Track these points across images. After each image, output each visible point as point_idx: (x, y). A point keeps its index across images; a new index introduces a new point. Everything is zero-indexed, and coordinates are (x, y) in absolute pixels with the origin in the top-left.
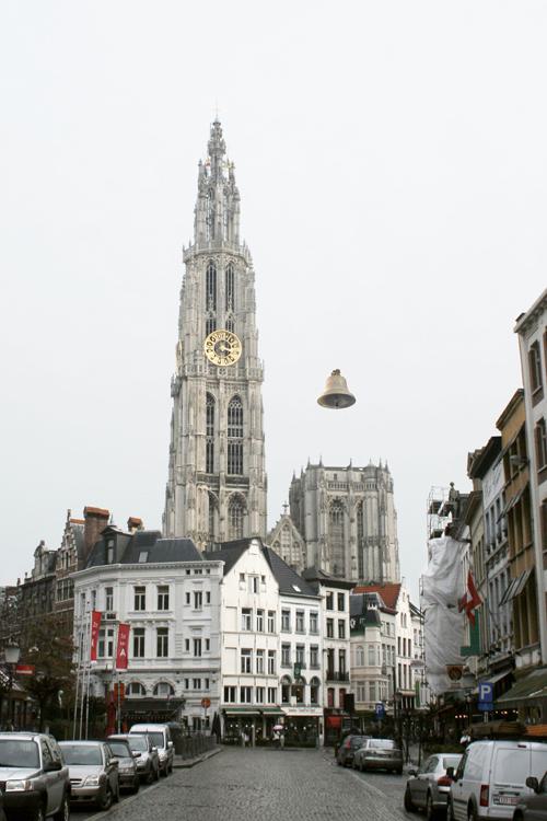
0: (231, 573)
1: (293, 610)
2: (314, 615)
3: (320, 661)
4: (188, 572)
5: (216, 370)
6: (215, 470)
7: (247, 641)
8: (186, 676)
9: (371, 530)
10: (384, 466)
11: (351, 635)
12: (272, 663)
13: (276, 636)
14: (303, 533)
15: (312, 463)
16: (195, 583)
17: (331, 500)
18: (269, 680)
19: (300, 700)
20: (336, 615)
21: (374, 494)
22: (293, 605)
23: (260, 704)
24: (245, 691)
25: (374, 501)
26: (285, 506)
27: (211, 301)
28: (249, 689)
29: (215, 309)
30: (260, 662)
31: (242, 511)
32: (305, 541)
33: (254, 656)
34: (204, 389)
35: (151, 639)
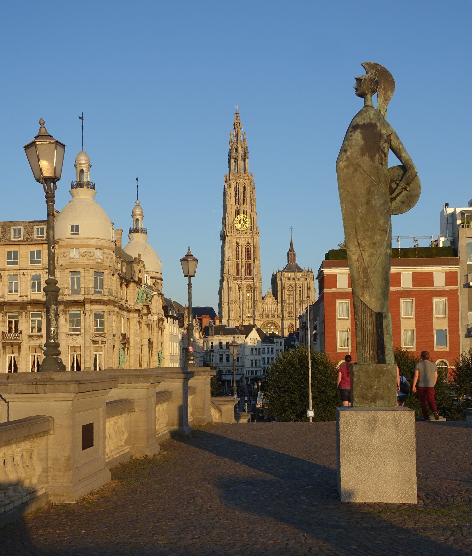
0: (247, 338)
2: (272, 348)
5: (240, 232)
6: (240, 274)
7: (253, 357)
10: (310, 270)
12: (260, 363)
13: (261, 355)
14: (276, 299)
15: (280, 270)
20: (279, 348)
21: (306, 282)
24: (252, 372)
25: (306, 285)
29: (239, 204)
30: (256, 363)
32: (277, 302)
33: (254, 362)
34: (235, 240)
35: (224, 357)
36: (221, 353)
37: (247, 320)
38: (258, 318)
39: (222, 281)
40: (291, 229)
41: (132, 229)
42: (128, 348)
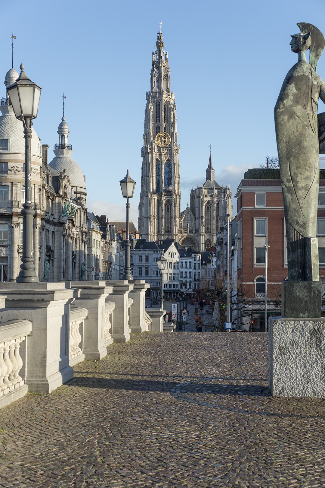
1: (184, 261)
2: (190, 263)
3: (192, 276)
4: (154, 252)
8: (154, 281)
9: (221, 214)
11: (202, 266)
12: (178, 277)
13: (179, 269)
14: (195, 215)
16: (156, 255)
17: (206, 202)
18: (177, 282)
19: (186, 287)
20: (197, 262)
22: (184, 260)
23: (174, 289)
24: (170, 285)
26: (188, 204)
27: (158, 119)
28: (171, 284)
31: (170, 206)
32: (195, 217)
35: (144, 270)
36: (140, 267)
37: (166, 235)
38: (176, 233)
39: (142, 196)
40: (211, 147)
41: (58, 145)
42: (53, 260)
